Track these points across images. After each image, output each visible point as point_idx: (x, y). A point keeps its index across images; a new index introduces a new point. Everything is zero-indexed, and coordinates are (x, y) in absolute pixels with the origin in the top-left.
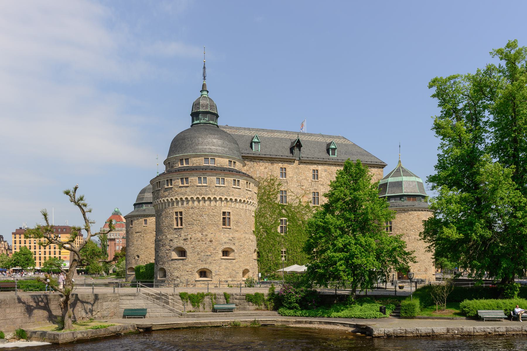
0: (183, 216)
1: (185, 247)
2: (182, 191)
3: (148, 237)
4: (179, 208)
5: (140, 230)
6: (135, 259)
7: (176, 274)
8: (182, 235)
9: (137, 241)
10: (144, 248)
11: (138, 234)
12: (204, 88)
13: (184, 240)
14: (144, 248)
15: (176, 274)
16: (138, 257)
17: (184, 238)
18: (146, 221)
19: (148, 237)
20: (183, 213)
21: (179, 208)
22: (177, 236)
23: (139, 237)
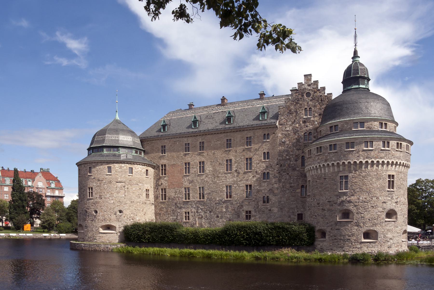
0: (395, 179)
1: (396, 210)
2: (398, 155)
3: (134, 189)
4: (392, 170)
5: (124, 180)
6: (115, 214)
7: (389, 235)
8: (394, 197)
9: (118, 193)
10: (128, 202)
11: (119, 185)
12: (356, 55)
13: (396, 202)
14: (128, 202)
15: (389, 235)
16: (121, 211)
17: (396, 201)
18: (109, 168)
19: (134, 189)
20: (395, 177)
21: (392, 170)
22: (390, 199)
23: (121, 188)
